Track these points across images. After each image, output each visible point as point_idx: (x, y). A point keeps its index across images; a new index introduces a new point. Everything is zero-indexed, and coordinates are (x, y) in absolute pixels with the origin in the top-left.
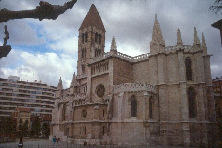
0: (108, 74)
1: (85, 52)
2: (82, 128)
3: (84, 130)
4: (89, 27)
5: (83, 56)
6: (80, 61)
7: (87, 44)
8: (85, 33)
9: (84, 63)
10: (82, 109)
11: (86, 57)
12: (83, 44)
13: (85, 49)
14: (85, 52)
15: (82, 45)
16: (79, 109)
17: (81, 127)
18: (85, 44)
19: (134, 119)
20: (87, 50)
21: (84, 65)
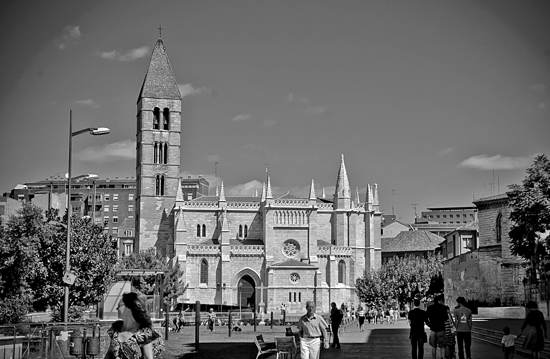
0: (308, 229)
1: (163, 149)
2: (293, 295)
3: (297, 296)
4: (176, 101)
5: (158, 158)
6: (152, 166)
7: (169, 136)
8: (162, 110)
9: (161, 172)
10: (290, 272)
11: (165, 163)
12: (159, 132)
13: (163, 144)
14: (163, 149)
15: (154, 132)
16: (282, 272)
17: (290, 293)
18: (165, 134)
19: (341, 285)
20: (170, 148)
21: (163, 176)
